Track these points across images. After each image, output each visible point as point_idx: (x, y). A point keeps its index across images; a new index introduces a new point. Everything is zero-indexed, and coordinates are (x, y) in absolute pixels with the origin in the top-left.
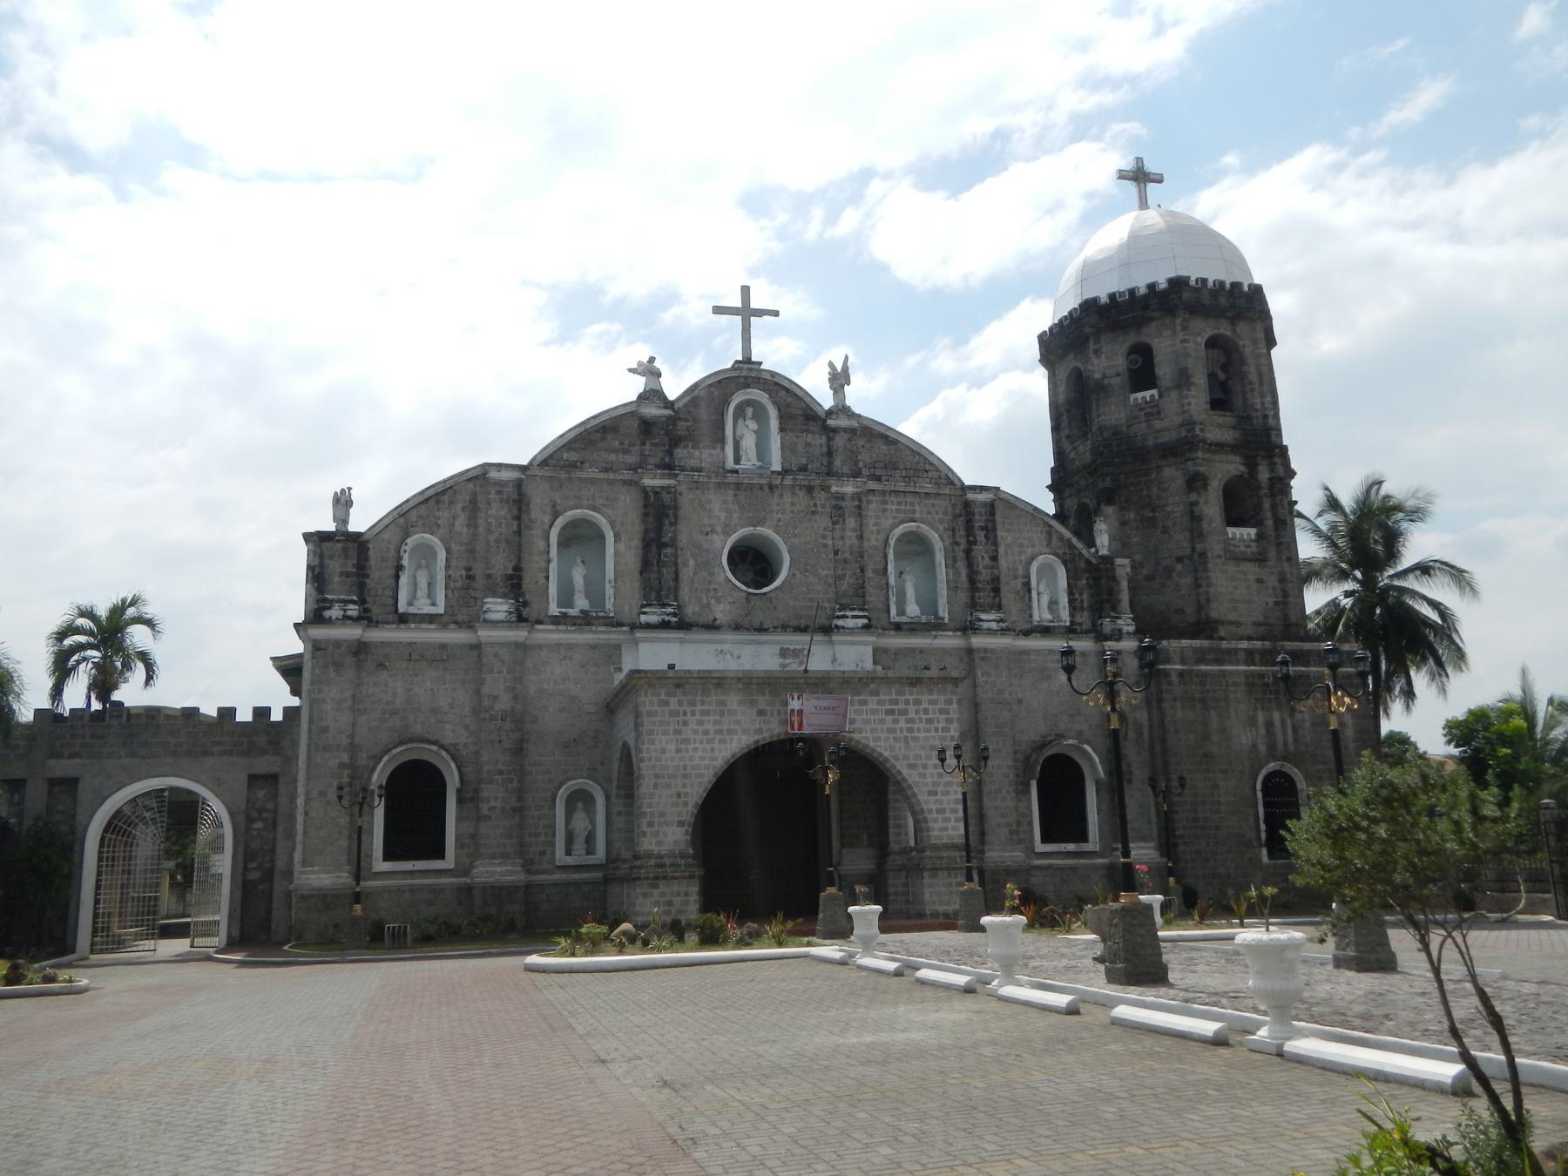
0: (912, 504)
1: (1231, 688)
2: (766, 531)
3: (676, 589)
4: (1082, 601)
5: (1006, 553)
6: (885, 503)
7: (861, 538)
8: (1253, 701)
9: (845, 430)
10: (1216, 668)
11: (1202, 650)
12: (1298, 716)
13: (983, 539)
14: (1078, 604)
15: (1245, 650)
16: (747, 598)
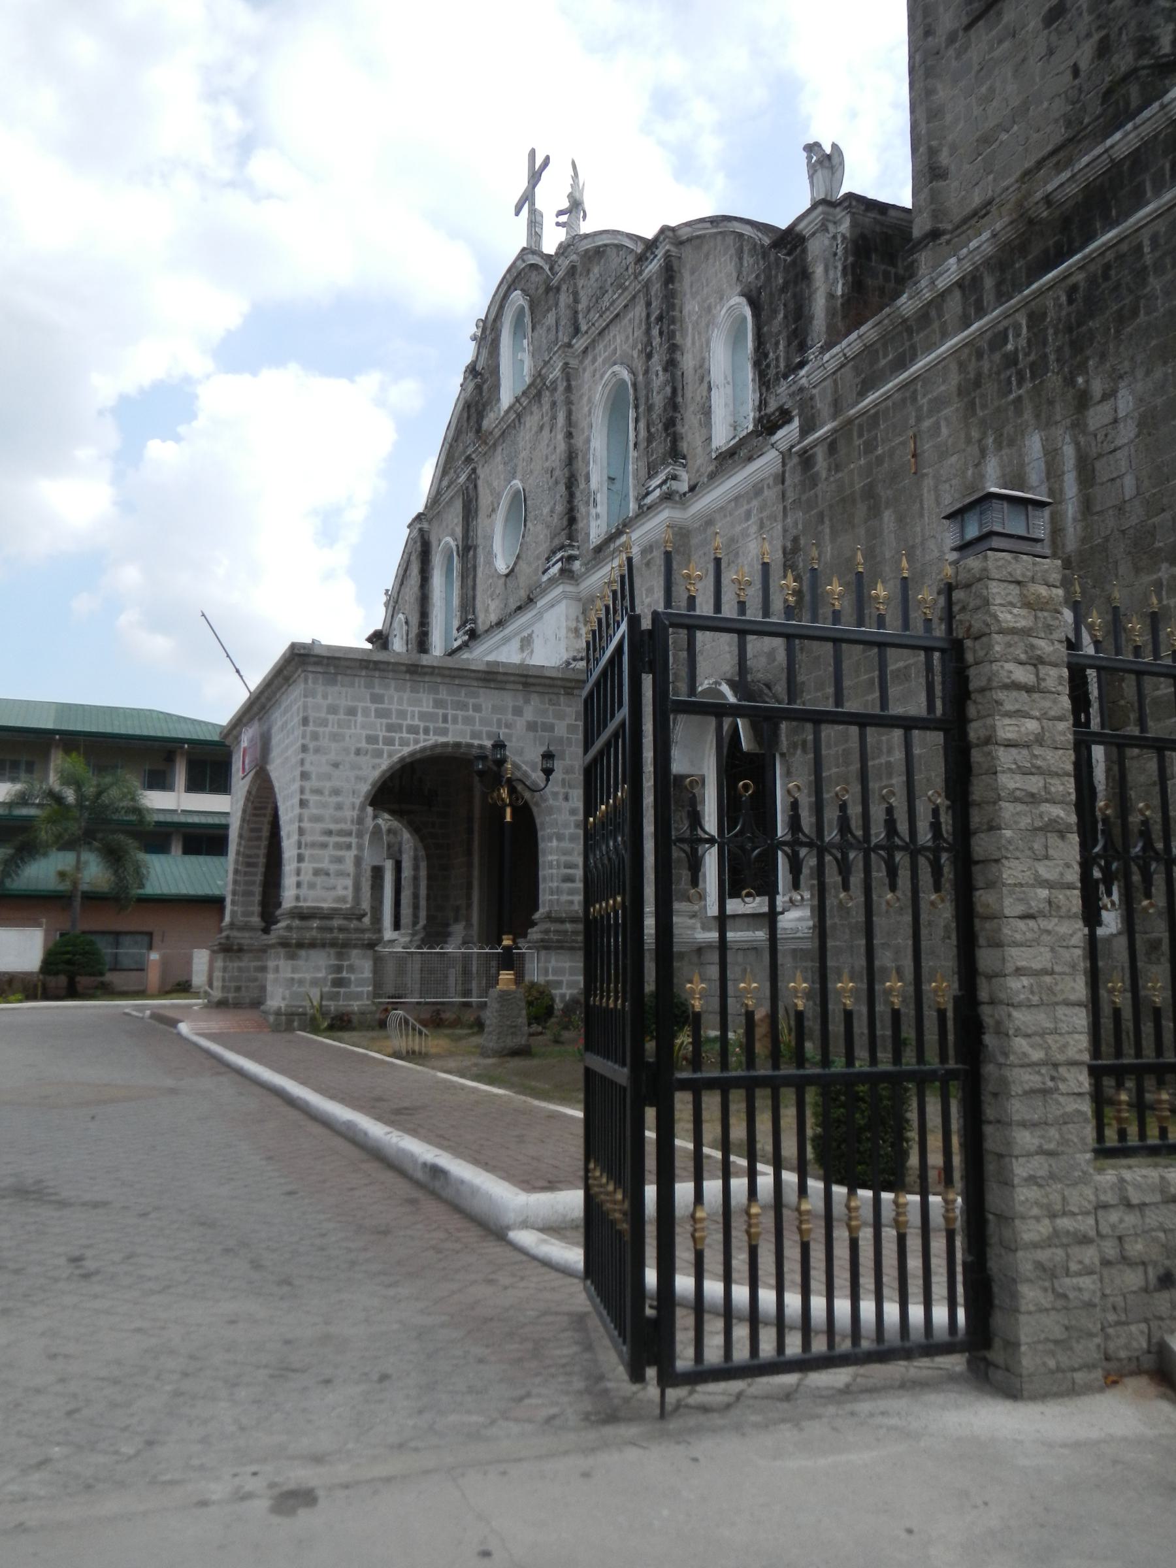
0: (615, 337)
1: (927, 424)
2: (517, 483)
3: (474, 598)
4: (777, 359)
5: (693, 343)
6: (594, 360)
7: (569, 435)
8: (975, 434)
9: (563, 279)
10: (890, 385)
11: (869, 352)
12: (1097, 417)
13: (658, 340)
14: (772, 372)
15: (960, 284)
16: (505, 584)
